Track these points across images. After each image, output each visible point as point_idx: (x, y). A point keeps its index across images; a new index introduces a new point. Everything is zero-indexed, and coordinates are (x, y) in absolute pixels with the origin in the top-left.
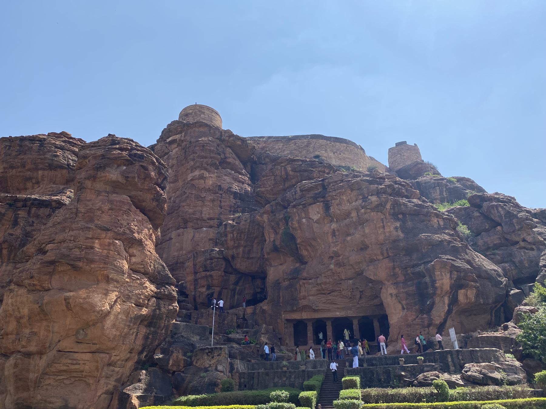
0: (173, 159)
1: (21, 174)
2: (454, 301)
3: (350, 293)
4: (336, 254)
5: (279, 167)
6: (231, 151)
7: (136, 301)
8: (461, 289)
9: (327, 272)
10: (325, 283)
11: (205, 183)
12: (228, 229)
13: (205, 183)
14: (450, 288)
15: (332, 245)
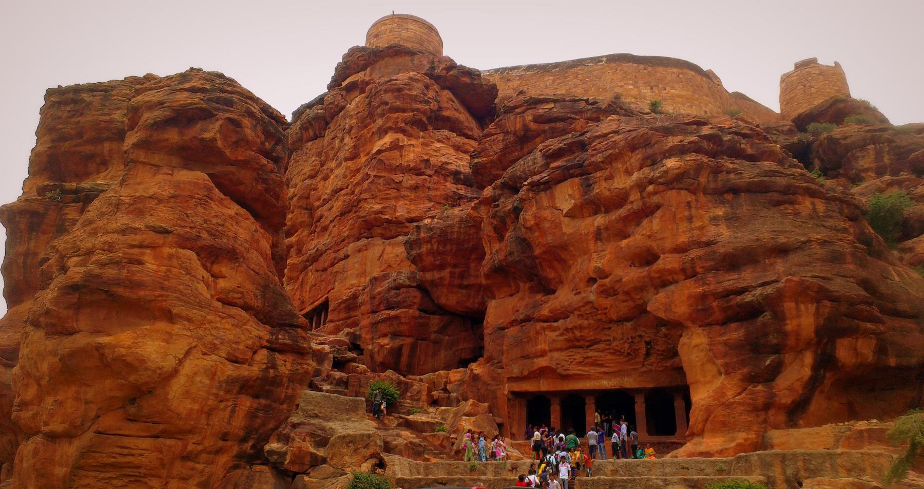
0: (351, 117)
1: (78, 149)
2: (825, 361)
3: (627, 346)
4: (602, 274)
5: (512, 117)
6: (450, 95)
7: (228, 354)
8: (843, 337)
9: (584, 306)
10: (581, 328)
11: (401, 156)
12: (422, 235)
13: (401, 156)
14: (818, 332)
15: (594, 256)
